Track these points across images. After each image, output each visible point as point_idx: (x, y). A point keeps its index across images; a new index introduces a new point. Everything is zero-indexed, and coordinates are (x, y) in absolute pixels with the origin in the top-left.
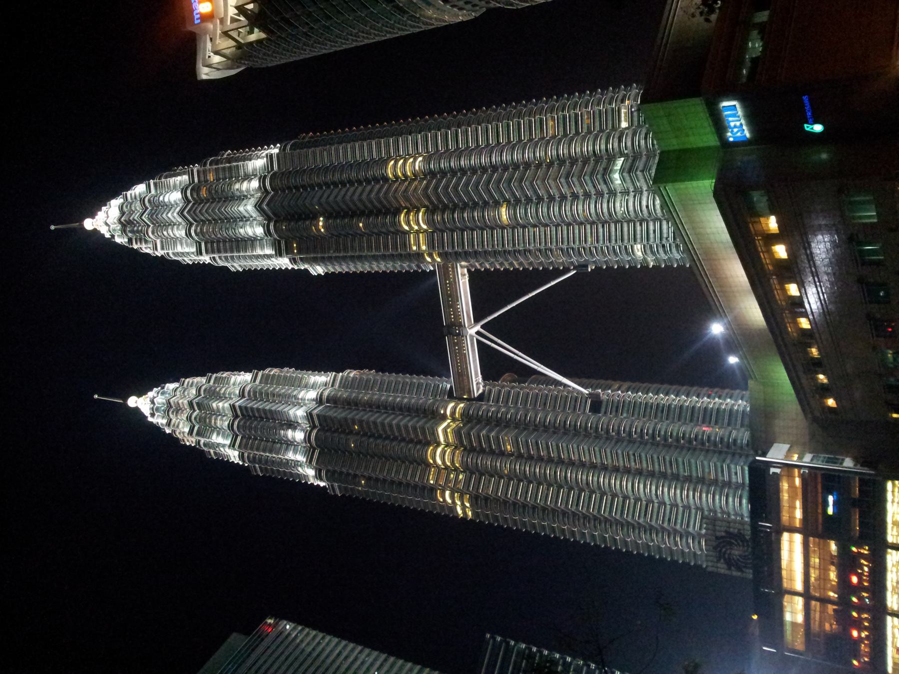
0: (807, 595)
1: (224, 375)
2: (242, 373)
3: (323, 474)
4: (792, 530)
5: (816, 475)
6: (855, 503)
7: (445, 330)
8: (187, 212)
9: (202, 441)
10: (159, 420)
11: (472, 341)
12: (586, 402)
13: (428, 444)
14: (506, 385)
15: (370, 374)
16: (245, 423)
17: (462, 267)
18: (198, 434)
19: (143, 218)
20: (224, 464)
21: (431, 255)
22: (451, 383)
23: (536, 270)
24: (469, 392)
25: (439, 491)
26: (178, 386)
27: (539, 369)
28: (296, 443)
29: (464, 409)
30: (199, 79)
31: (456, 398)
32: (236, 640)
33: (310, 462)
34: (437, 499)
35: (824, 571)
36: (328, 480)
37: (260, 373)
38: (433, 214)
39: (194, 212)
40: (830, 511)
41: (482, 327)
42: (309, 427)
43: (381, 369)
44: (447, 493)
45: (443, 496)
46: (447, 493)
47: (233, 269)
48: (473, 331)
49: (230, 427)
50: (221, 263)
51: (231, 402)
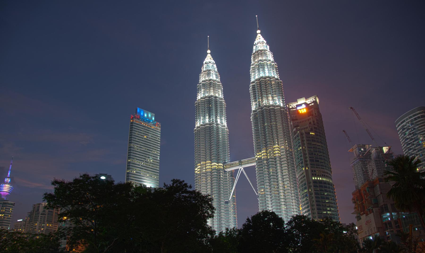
3: (199, 129)
12: (228, 200)
38: (266, 160)
44: (200, 167)
46: (200, 167)
48: (241, 168)
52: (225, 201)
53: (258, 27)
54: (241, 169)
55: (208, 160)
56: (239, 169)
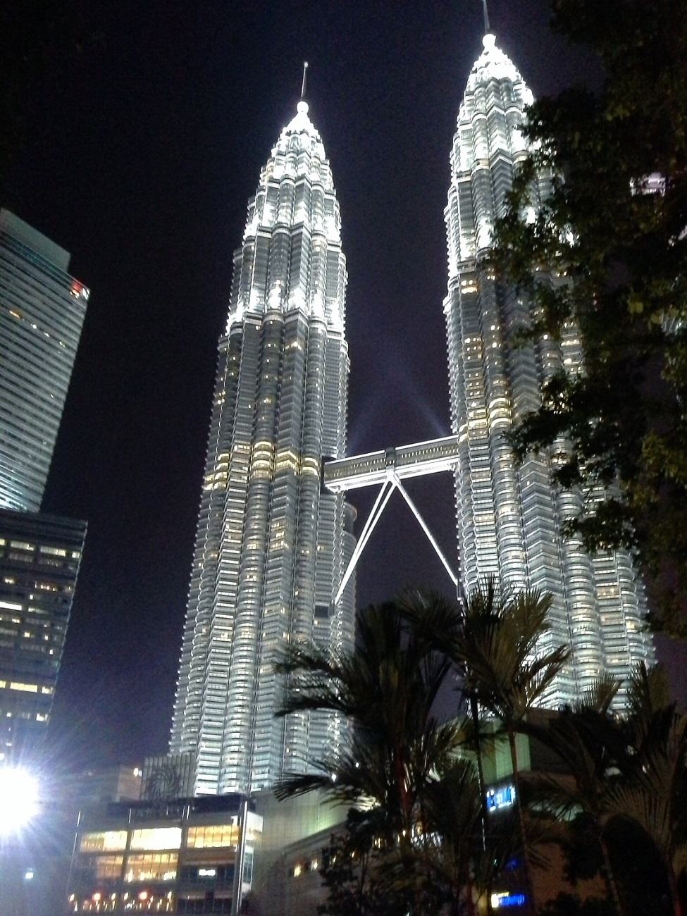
0: (127, 853)
1: (335, 208)
2: (340, 227)
3: (239, 331)
4: (184, 836)
5: (233, 858)
6: (210, 895)
7: (390, 449)
8: (501, 160)
9: (264, 193)
10: (283, 142)
12: (328, 602)
13: (274, 441)
14: (341, 511)
15: (344, 367)
16: (285, 241)
18: (271, 189)
19: (495, 108)
20: (241, 219)
21: (465, 431)
23: (457, 542)
24: (329, 479)
25: (227, 455)
26: (321, 159)
27: (356, 550)
28: (267, 298)
29: (312, 475)
31: (323, 464)
32: (62, 257)
33: (248, 317)
34: (220, 453)
35: (150, 867)
36: (232, 336)
37: (338, 250)
39: (502, 168)
40: (202, 872)
41: (396, 487)
42: (284, 312)
43: (353, 380)
45: (223, 460)
47: (446, 210)
48: (392, 477)
49: (280, 225)
50: (450, 199)
51: (306, 223)
52: (316, 606)
53: (487, 25)
54: (390, 484)
55: (264, 438)
56: (383, 484)
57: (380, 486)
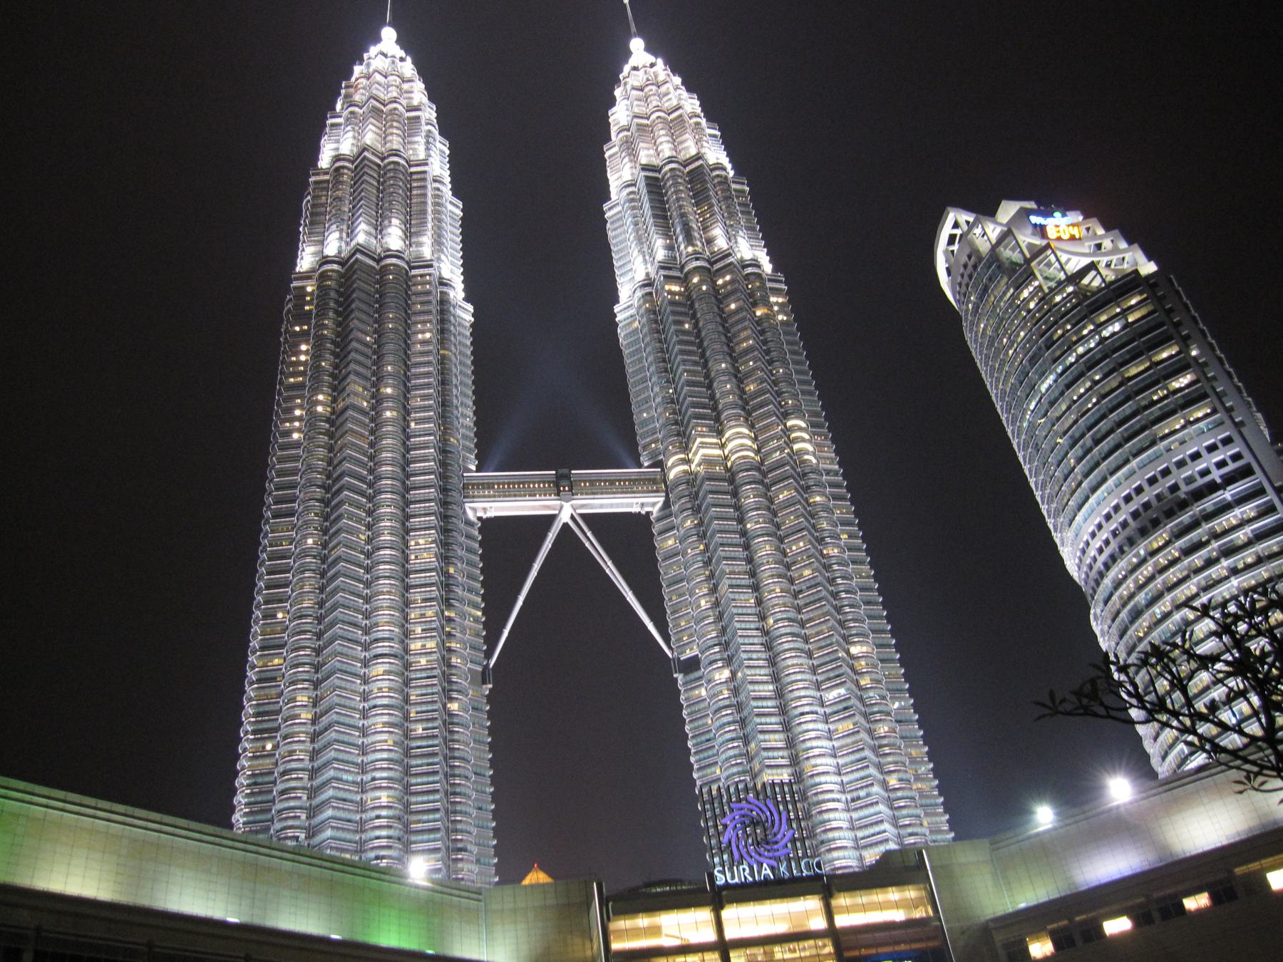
3: (335, 267)
7: (565, 471)
11: (548, 507)
17: (654, 504)
22: (477, 471)
28: (379, 237)
30: (949, 209)
41: (566, 526)
49: (396, 153)
53: (633, 29)
57: (550, 519)
